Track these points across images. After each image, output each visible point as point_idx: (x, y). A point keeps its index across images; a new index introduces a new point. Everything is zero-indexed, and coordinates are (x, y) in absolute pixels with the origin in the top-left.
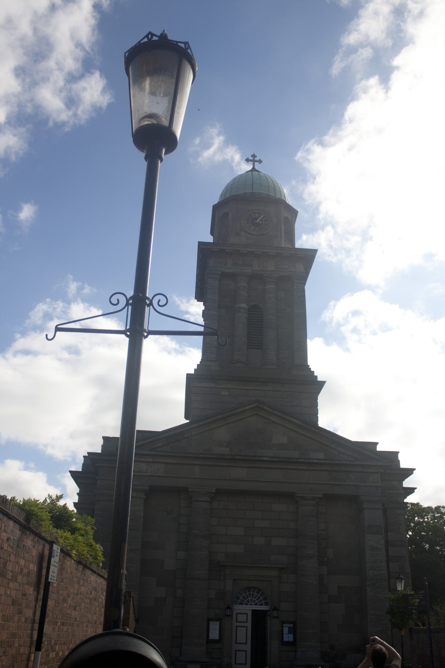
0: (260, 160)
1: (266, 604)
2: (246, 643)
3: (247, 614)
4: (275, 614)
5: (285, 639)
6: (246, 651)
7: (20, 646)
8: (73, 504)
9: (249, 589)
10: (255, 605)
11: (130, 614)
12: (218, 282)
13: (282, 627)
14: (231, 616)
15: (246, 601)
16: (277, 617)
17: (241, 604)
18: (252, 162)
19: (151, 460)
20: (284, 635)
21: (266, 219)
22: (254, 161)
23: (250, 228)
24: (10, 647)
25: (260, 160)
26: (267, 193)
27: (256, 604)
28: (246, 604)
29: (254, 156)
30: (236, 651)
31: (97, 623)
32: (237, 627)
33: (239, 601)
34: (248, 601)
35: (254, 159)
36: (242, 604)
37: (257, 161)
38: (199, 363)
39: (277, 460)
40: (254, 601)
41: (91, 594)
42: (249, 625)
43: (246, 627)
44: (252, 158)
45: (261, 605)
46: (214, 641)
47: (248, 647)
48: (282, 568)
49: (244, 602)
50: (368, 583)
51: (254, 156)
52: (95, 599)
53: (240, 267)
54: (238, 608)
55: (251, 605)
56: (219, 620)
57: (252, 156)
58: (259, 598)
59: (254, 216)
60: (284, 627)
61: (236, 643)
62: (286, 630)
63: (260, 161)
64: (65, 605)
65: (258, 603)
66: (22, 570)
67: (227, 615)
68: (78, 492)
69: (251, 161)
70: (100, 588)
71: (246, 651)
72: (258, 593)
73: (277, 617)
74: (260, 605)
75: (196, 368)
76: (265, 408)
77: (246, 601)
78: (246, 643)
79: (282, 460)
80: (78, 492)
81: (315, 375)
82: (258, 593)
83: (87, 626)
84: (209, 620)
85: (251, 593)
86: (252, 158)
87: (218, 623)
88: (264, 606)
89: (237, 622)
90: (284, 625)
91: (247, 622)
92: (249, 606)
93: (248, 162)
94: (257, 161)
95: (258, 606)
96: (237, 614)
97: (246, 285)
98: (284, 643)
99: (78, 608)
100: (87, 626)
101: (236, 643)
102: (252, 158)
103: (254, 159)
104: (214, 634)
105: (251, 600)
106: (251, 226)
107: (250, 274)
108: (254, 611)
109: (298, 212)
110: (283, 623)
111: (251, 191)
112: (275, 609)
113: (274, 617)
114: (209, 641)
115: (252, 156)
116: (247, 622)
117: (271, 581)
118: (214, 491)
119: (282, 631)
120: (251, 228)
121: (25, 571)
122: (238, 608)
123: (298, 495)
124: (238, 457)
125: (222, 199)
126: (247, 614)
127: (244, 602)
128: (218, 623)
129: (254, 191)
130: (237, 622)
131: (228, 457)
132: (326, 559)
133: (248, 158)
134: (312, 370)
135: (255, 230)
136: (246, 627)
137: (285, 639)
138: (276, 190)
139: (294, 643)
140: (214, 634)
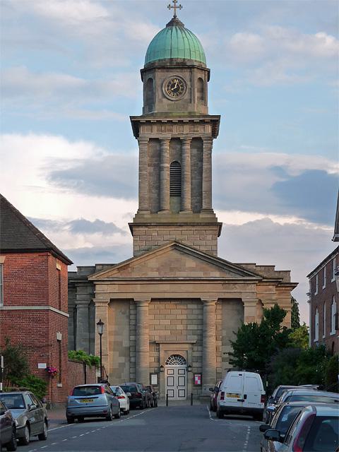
1: (185, 364)
9: (175, 356)
22: (175, 7)
62: (196, 379)
63: (180, 7)
84: (151, 374)
103: (175, 5)
110: (194, 374)
119: (194, 378)
139: (201, 385)
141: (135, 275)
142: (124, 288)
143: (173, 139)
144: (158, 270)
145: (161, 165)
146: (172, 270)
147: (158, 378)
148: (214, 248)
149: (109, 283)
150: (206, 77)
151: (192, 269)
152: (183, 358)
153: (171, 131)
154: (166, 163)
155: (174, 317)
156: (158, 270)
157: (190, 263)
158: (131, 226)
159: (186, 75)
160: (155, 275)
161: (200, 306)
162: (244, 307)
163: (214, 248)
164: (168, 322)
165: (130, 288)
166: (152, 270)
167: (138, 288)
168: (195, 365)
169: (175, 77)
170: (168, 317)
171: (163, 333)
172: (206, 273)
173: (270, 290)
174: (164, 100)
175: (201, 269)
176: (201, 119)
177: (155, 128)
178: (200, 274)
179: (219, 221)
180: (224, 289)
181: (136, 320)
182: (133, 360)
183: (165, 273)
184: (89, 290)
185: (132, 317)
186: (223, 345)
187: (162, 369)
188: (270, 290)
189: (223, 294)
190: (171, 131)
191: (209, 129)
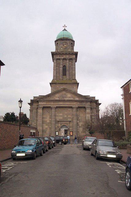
4: (69, 130)
9: (64, 125)
29: (65, 25)
46: (57, 135)
51: (65, 25)
63: (66, 27)
139: (72, 135)
141: (52, 99)
142: (48, 103)
143: (64, 59)
151: (70, 97)
157: (69, 95)
159: (68, 42)
165: (50, 103)
167: (52, 103)
168: (70, 128)
171: (60, 118)
175: (72, 97)
177: (58, 56)
178: (72, 99)
179: (78, 82)
184: (37, 104)
186: (79, 122)
187: (60, 130)
191: (74, 56)
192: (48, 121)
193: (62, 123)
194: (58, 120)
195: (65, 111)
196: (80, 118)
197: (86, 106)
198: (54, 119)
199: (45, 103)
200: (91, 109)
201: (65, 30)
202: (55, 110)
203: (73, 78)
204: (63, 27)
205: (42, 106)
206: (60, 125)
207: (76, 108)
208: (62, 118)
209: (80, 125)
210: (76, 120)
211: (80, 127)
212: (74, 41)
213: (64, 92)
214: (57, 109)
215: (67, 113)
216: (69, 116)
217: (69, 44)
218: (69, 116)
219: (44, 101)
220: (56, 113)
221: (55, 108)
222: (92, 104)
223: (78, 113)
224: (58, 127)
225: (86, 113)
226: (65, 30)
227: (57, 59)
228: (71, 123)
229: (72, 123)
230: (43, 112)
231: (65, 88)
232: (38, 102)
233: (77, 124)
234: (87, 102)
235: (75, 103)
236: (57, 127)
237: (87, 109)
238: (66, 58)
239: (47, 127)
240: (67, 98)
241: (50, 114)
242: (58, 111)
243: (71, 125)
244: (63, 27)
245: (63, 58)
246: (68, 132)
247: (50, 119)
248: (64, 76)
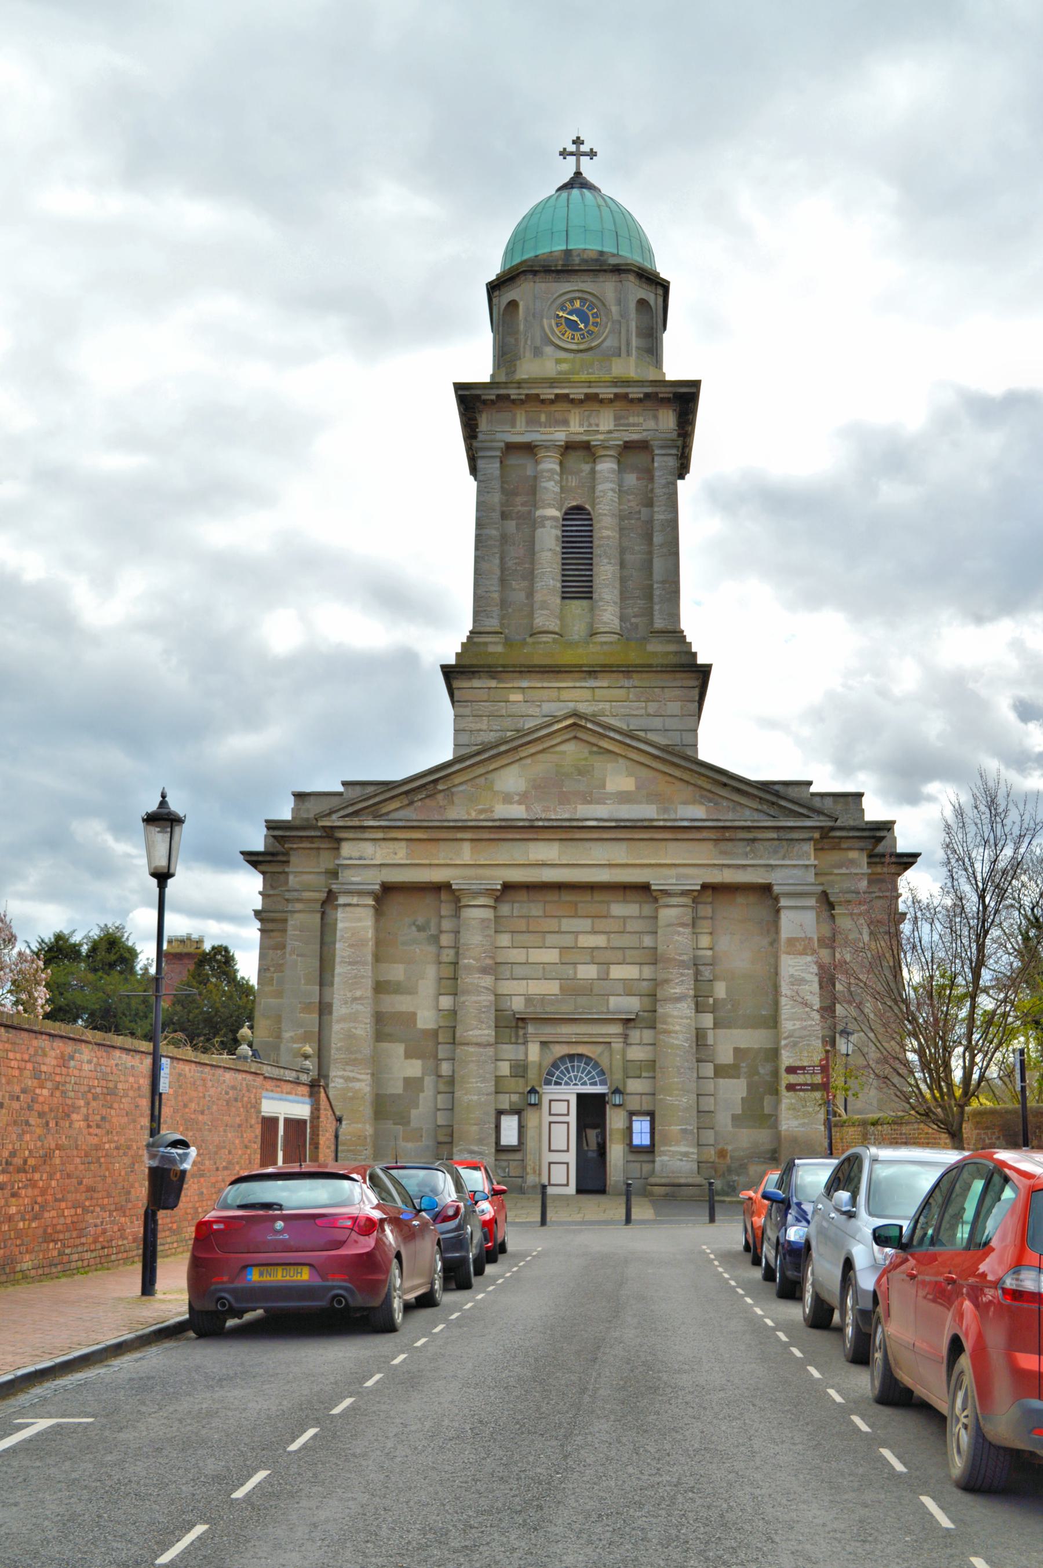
0: (591, 150)
1: (603, 1083)
2: (568, 1151)
3: (568, 1101)
4: (617, 1099)
5: (636, 1141)
6: (567, 1164)
7: (138, 1148)
8: (253, 913)
9: (571, 1057)
10: (582, 1084)
11: (321, 1111)
12: (498, 465)
13: (631, 1122)
14: (537, 1105)
15: (566, 1079)
16: (620, 1105)
17: (557, 1083)
18: (574, 158)
19: (380, 835)
20: (634, 1136)
21: (595, 310)
22: (578, 154)
23: (563, 335)
24: (129, 1149)
25: (591, 150)
26: (600, 249)
27: (584, 1084)
28: (567, 1084)
29: (578, 142)
30: (550, 1163)
31: (244, 1126)
32: (550, 1123)
33: (554, 1079)
34: (570, 1078)
35: (578, 148)
36: (560, 1084)
37: (585, 154)
38: (465, 640)
39: (613, 824)
40: (581, 1078)
41: (227, 1093)
42: (573, 1119)
43: (568, 1123)
44: (572, 148)
45: (594, 1084)
47: (571, 1157)
48: (629, 1020)
49: (562, 1079)
50: (783, 1042)
51: (578, 142)
52: (236, 1100)
53: (542, 429)
54: (549, 1092)
55: (575, 1084)
56: (518, 1112)
57: (574, 142)
58: (589, 1072)
59: (571, 307)
60: (634, 1123)
61: (550, 1150)
63: (592, 154)
64: (187, 1110)
65: (588, 1082)
66: (132, 1086)
67: (531, 1105)
68: (261, 890)
69: (572, 154)
70: (244, 1085)
71: (567, 1164)
72: (587, 1064)
73: (620, 1105)
74: (591, 1084)
75: (459, 650)
76: (589, 725)
77: (566, 1079)
78: (568, 1151)
79: (622, 824)
80: (261, 890)
81: (693, 650)
82: (587, 1064)
83: (225, 1131)
84: (500, 1113)
85: (576, 1064)
86: (575, 146)
87: (516, 1117)
88: (599, 1087)
89: (550, 1114)
90: (634, 1118)
91: (568, 1115)
92: (571, 1087)
93: (565, 158)
94: (585, 154)
95: (589, 1087)
96: (550, 1101)
97: (557, 468)
98: (634, 1150)
99: (206, 1112)
100: (225, 1131)
101: (550, 1150)
102: (572, 148)
103: (578, 148)
104: (509, 1135)
105: (576, 1077)
106: (566, 331)
107: (563, 443)
108: (580, 1097)
109: (668, 283)
110: (632, 1114)
111: (564, 247)
112: (616, 1091)
113: (615, 1105)
114: (501, 1150)
115: (574, 142)
116: (568, 1115)
117: (610, 1043)
118: (499, 887)
119: (629, 1129)
120: (566, 336)
121: (136, 1086)
122: (549, 1092)
123: (653, 887)
124: (540, 824)
125: (507, 268)
126: (568, 1101)
127: (562, 1079)
128: (516, 1117)
129: (570, 248)
130: (550, 1114)
131: (521, 824)
132: (711, 1000)
133: (565, 149)
134: (688, 640)
135: (573, 339)
136: (568, 1123)
137: (636, 1141)
138: (619, 238)
139: (650, 1150)
140: (509, 1135)
141: (457, 813)
142: (425, 854)
143: (569, 447)
144: (524, 798)
145: (539, 513)
146: (564, 799)
147: (521, 1128)
148: (687, 738)
149: (380, 835)
150: (660, 300)
151: (624, 798)
152: (596, 1065)
153: (565, 423)
154: (550, 506)
155: (567, 940)
156: (524, 798)
158: (449, 673)
159: (607, 288)
160: (517, 811)
161: (647, 909)
162: (778, 911)
163: (687, 738)
164: (551, 956)
165: (443, 854)
166: (507, 799)
167: (466, 853)
168: (634, 1086)
169: (577, 295)
170: (551, 939)
171: (537, 988)
172: (666, 810)
173: (852, 862)
174: (549, 350)
175: (652, 798)
176: (649, 390)
178: (647, 811)
179: (700, 660)
180: (724, 853)
181: (456, 947)
182: (445, 1068)
183: (546, 809)
184: (326, 861)
185: (446, 940)
186: (716, 1025)
187: (533, 1099)
188: (852, 862)
189: (716, 871)
190: (565, 423)
191: (667, 420)
192: (426, 1019)
193: (549, 1031)
194: (518, 1005)
195: (585, 924)
196: (720, 990)
197: (777, 879)
198: (487, 998)
199: (398, 853)
200: (827, 903)
201: (578, 181)
202: (488, 914)
203: (659, 624)
204: (564, 153)
205: (374, 880)
206: (534, 1052)
207: (684, 893)
208: (552, 988)
209: (725, 1056)
210: (686, 1008)
211: (721, 1071)
212: (663, 287)
213: (571, 751)
214: (505, 909)
215: (600, 941)
216: (618, 972)
217: (614, 309)
218: (618, 972)
219: (389, 832)
220: (504, 940)
221: (488, 892)
222: (834, 857)
223: (705, 941)
224: (520, 1069)
225: (774, 942)
226: (578, 181)
227: (511, 448)
228: (635, 1035)
229: (648, 1035)
230: (377, 930)
231: (584, 708)
232: (332, 837)
233: (700, 1037)
234: (785, 837)
235: (675, 853)
236: (505, 1069)
237: (783, 902)
238: (596, 439)
239: (414, 1068)
240: (601, 801)
241: (448, 955)
242: (522, 925)
243: (637, 1053)
244: (564, 153)
245: (560, 436)
246: (615, 1120)
247: (446, 1002)
248: (577, 607)
